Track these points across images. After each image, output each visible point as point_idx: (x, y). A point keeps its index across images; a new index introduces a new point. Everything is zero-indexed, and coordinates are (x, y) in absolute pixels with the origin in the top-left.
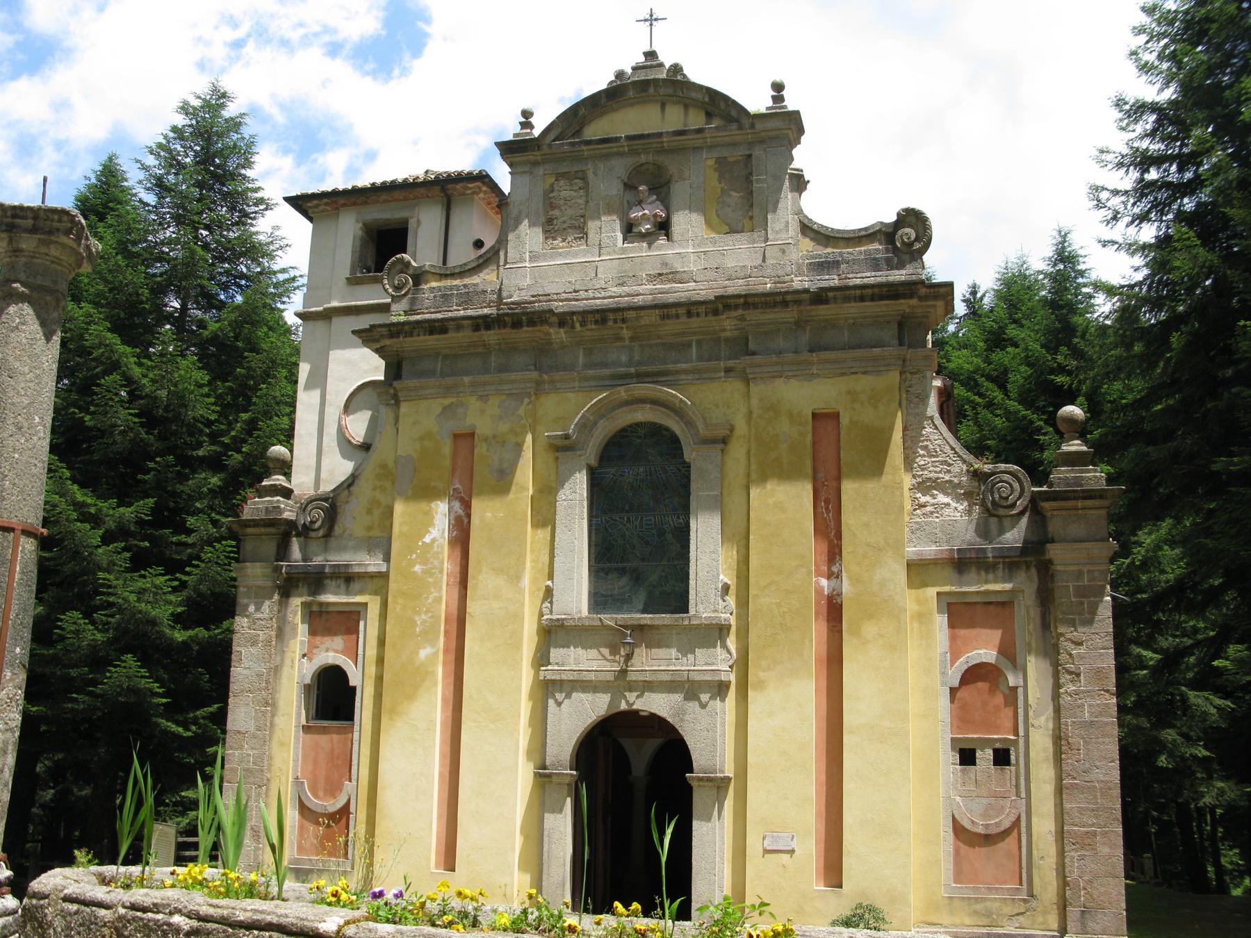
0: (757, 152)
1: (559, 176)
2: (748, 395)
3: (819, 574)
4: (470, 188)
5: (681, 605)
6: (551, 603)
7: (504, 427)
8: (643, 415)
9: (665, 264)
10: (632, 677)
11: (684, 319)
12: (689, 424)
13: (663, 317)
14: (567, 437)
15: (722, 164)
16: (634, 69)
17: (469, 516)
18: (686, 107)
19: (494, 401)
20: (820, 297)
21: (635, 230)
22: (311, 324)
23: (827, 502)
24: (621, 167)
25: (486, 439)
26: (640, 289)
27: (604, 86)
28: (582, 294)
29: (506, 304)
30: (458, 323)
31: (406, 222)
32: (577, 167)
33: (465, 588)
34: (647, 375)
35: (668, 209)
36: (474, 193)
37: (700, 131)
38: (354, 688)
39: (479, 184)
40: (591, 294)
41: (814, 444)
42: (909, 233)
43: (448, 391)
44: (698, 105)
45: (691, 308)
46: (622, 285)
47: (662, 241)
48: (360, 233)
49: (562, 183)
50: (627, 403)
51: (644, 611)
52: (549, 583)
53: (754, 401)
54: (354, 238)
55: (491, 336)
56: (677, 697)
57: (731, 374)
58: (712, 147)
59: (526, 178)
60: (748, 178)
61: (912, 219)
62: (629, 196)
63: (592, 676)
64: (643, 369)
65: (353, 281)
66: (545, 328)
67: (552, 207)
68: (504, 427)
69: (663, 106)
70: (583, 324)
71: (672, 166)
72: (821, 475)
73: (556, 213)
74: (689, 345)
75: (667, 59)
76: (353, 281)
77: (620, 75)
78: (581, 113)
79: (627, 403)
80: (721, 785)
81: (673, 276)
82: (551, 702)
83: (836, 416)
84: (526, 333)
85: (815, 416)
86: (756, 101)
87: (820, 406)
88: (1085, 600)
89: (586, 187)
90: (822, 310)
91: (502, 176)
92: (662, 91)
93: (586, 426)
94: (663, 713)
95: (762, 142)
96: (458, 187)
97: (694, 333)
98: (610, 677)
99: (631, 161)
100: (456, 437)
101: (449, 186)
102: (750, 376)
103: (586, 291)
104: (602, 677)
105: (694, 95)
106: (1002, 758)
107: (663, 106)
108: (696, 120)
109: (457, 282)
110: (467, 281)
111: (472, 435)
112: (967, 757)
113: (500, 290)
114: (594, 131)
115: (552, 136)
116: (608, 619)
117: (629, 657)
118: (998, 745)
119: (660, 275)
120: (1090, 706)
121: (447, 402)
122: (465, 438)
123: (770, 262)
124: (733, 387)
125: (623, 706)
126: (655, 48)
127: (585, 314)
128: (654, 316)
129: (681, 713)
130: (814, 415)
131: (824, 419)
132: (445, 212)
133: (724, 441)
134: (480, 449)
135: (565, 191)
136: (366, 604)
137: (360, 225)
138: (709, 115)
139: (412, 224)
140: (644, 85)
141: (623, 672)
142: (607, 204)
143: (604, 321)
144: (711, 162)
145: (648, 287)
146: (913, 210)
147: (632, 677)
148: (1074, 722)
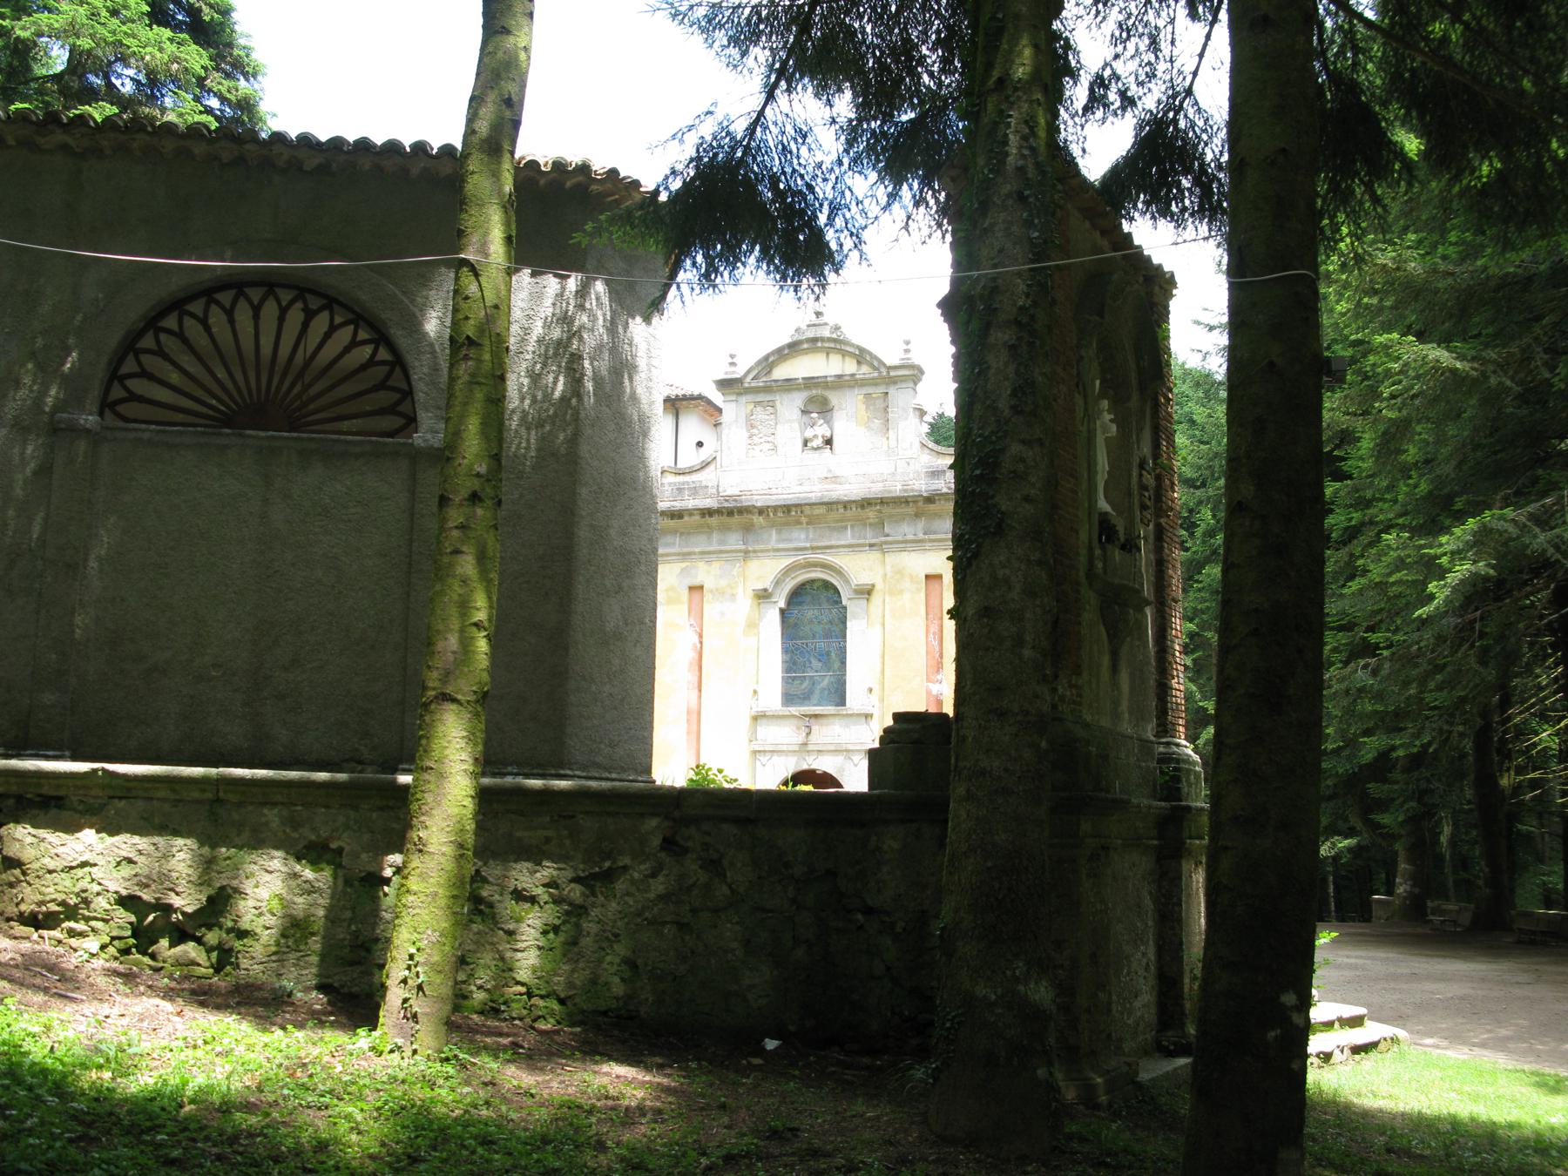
0: (892, 391)
1: (757, 404)
2: (884, 562)
3: (928, 680)
5: (842, 701)
7: (723, 583)
8: (817, 574)
9: (830, 471)
10: (810, 748)
11: (842, 510)
12: (847, 581)
13: (831, 510)
14: (765, 590)
15: (868, 395)
17: (701, 643)
19: (716, 565)
20: (930, 500)
23: (934, 634)
24: (798, 399)
25: (711, 591)
26: (814, 489)
28: (774, 491)
30: (690, 512)
32: (769, 398)
33: (700, 691)
34: (818, 548)
35: (831, 429)
37: (853, 375)
41: (927, 595)
43: (685, 556)
44: (851, 355)
45: (846, 505)
49: (758, 409)
50: (804, 566)
53: (888, 568)
55: (714, 521)
56: (840, 759)
58: (862, 385)
60: (886, 409)
62: (805, 418)
63: (785, 748)
64: (815, 544)
66: (750, 516)
67: (752, 426)
68: (723, 583)
69: (828, 354)
70: (775, 513)
71: (834, 398)
73: (755, 431)
74: (846, 528)
78: (771, 359)
79: (804, 566)
81: (835, 479)
82: (758, 763)
84: (736, 518)
85: (927, 577)
87: (931, 571)
89: (775, 413)
90: (932, 507)
91: (717, 397)
92: (827, 345)
93: (778, 583)
95: (895, 383)
99: (804, 395)
100: (691, 588)
107: (828, 354)
108: (850, 367)
109: (686, 478)
111: (701, 587)
114: (781, 372)
115: (751, 376)
116: (794, 710)
117: (808, 734)
121: (684, 565)
122: (697, 589)
123: (899, 470)
125: (805, 767)
127: (776, 508)
128: (821, 510)
129: (842, 770)
130: (927, 577)
133: (869, 592)
134: (707, 596)
135: (761, 415)
138: (859, 363)
140: (814, 340)
141: (805, 744)
143: (789, 511)
144: (861, 397)
147: (810, 748)
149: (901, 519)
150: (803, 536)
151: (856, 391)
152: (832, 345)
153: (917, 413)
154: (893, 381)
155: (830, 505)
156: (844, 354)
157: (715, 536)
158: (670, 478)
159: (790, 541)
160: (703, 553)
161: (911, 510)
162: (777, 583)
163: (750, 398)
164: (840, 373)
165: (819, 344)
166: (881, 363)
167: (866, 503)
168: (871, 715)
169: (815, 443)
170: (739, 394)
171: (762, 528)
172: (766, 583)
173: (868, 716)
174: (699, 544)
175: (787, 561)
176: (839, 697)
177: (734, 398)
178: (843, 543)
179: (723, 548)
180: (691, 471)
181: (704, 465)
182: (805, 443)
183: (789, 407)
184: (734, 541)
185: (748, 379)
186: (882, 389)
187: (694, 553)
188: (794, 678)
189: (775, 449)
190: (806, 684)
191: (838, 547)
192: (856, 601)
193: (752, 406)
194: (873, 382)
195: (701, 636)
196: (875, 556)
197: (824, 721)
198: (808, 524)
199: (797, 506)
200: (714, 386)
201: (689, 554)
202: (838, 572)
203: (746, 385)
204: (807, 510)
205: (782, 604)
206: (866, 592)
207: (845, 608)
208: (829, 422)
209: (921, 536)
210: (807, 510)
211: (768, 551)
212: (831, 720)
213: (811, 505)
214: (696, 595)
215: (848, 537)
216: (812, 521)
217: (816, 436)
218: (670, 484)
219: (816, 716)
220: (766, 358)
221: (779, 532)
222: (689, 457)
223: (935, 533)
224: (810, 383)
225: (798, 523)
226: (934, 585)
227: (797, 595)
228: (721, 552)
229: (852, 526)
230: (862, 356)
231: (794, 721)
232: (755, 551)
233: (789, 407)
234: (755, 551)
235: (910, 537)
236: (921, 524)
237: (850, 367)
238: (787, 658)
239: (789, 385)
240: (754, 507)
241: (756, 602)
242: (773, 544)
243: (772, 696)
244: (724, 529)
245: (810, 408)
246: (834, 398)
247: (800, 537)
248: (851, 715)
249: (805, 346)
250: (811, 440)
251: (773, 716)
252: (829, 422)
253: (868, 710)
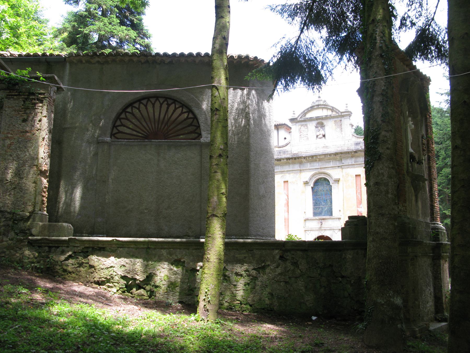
0: (343, 119)
5: (331, 214)
11: (329, 156)
12: (332, 178)
14: (307, 181)
17: (288, 198)
18: (327, 109)
19: (292, 175)
20: (356, 152)
23: (359, 193)
24: (314, 123)
30: (283, 159)
34: (322, 168)
40: (310, 151)
41: (356, 181)
45: (330, 155)
47: (324, 138)
49: (302, 127)
51: (324, 216)
55: (290, 161)
62: (317, 129)
63: (314, 229)
66: (301, 159)
69: (322, 109)
71: (325, 122)
72: (357, 188)
74: (331, 162)
81: (327, 147)
85: (356, 176)
86: (342, 109)
89: (307, 128)
90: (356, 154)
91: (289, 124)
92: (322, 106)
93: (310, 179)
95: (343, 117)
97: (331, 159)
98: (318, 229)
99: (316, 122)
100: (284, 182)
105: (329, 107)
107: (322, 109)
108: (329, 113)
109: (281, 149)
110: (284, 148)
111: (287, 181)
114: (309, 116)
115: (300, 117)
116: (317, 218)
122: (286, 182)
125: (320, 234)
127: (309, 157)
128: (323, 157)
130: (356, 176)
138: (332, 111)
140: (318, 105)
144: (333, 122)
147: (322, 229)
149: (347, 158)
151: (332, 120)
152: (324, 106)
153: (351, 126)
154: (343, 116)
155: (325, 155)
156: (327, 109)
157: (291, 166)
158: (277, 149)
159: (314, 166)
161: (350, 155)
162: (310, 179)
163: (299, 124)
164: (326, 115)
165: (320, 106)
166: (339, 111)
167: (336, 154)
168: (340, 218)
170: (296, 123)
171: (305, 163)
172: (307, 179)
173: (339, 219)
174: (286, 168)
175: (313, 173)
176: (330, 212)
177: (295, 124)
178: (330, 166)
180: (283, 147)
181: (287, 145)
182: (317, 136)
183: (312, 125)
184: (297, 167)
185: (299, 118)
186: (340, 119)
187: (285, 171)
188: (316, 208)
189: (308, 139)
190: (320, 209)
191: (328, 167)
192: (334, 184)
193: (300, 126)
194: (337, 117)
195: (288, 196)
196: (340, 170)
197: (326, 220)
198: (319, 161)
199: (316, 156)
200: (289, 121)
201: (283, 171)
202: (329, 175)
203: (298, 120)
204: (319, 157)
205: (312, 186)
206: (337, 181)
207: (331, 186)
208: (324, 130)
209: (353, 163)
210: (319, 157)
211: (307, 170)
212: (328, 220)
213: (320, 155)
214: (286, 184)
215: (331, 164)
216: (320, 160)
217: (320, 134)
218: (277, 151)
219: (323, 219)
220: (304, 111)
221: (310, 164)
222: (282, 143)
223: (358, 162)
224: (317, 118)
225: (316, 161)
226: (358, 178)
227: (316, 183)
228: (293, 170)
230: (333, 109)
231: (317, 221)
232: (303, 170)
233: (312, 125)
234: (303, 170)
235: (350, 164)
236: (353, 160)
237: (329, 113)
238: (314, 202)
239: (311, 119)
240: (302, 157)
241: (304, 185)
242: (309, 167)
243: (310, 214)
244: (294, 163)
245: (318, 126)
246: (325, 122)
247: (317, 165)
248: (334, 218)
249: (316, 107)
250: (319, 136)
251: (311, 220)
252: (324, 130)
253: (340, 217)
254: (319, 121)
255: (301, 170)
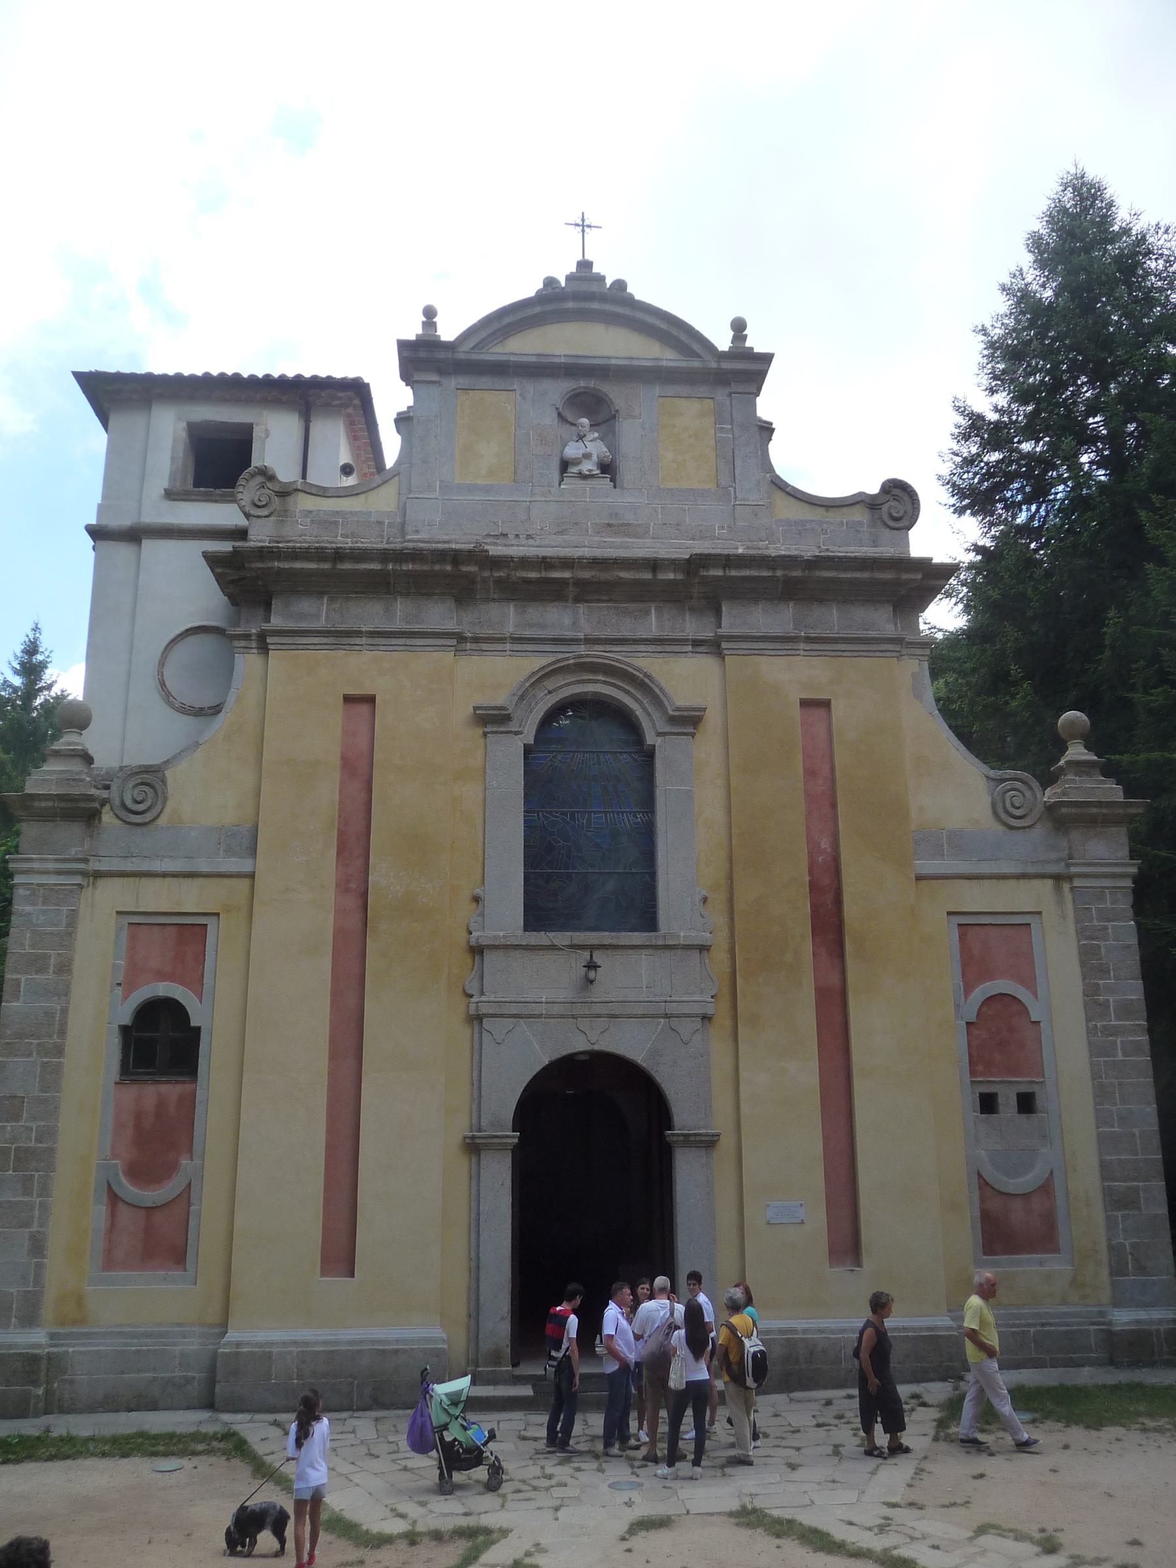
4: (340, 399)
5: (650, 922)
6: (482, 915)
12: (657, 702)
16: (569, 278)
21: (574, 470)
22: (107, 546)
24: (556, 390)
27: (530, 293)
29: (409, 541)
31: (248, 429)
36: (341, 406)
38: (198, 1030)
39: (350, 394)
42: (897, 508)
46: (562, 533)
48: (183, 435)
52: (478, 891)
54: (175, 440)
57: (701, 649)
59: (434, 391)
61: (896, 491)
62: (564, 431)
63: (543, 1009)
65: (170, 495)
74: (648, 613)
75: (609, 270)
76: (170, 495)
77: (550, 282)
80: (709, 1143)
83: (826, 704)
85: (805, 704)
88: (1110, 924)
94: (638, 1056)
96: (323, 394)
101: (312, 392)
102: (725, 652)
103: (517, 536)
104: (556, 1009)
106: (1026, 1103)
111: (370, 700)
112: (988, 1104)
113: (403, 524)
115: (471, 343)
118: (1024, 1089)
119: (609, 525)
120: (1122, 1042)
123: (740, 524)
124: (705, 664)
126: (588, 257)
131: (816, 705)
132: (302, 424)
136: (218, 914)
137: (184, 424)
139: (257, 433)
142: (540, 435)
145: (596, 539)
146: (901, 481)
148: (1107, 1062)
150: (567, 621)
160: (373, 634)
162: (522, 698)
169: (587, 467)
172: (501, 699)
173: (703, 948)
175: (537, 662)
179: (416, 627)
182: (565, 465)
187: (358, 633)
202: (643, 685)
203: (461, 356)
211: (502, 640)
217: (587, 456)
229: (658, 610)
232: (476, 640)
234: (476, 640)
250: (577, 462)
253: (703, 937)
254: (582, 384)
255: (461, 638)
